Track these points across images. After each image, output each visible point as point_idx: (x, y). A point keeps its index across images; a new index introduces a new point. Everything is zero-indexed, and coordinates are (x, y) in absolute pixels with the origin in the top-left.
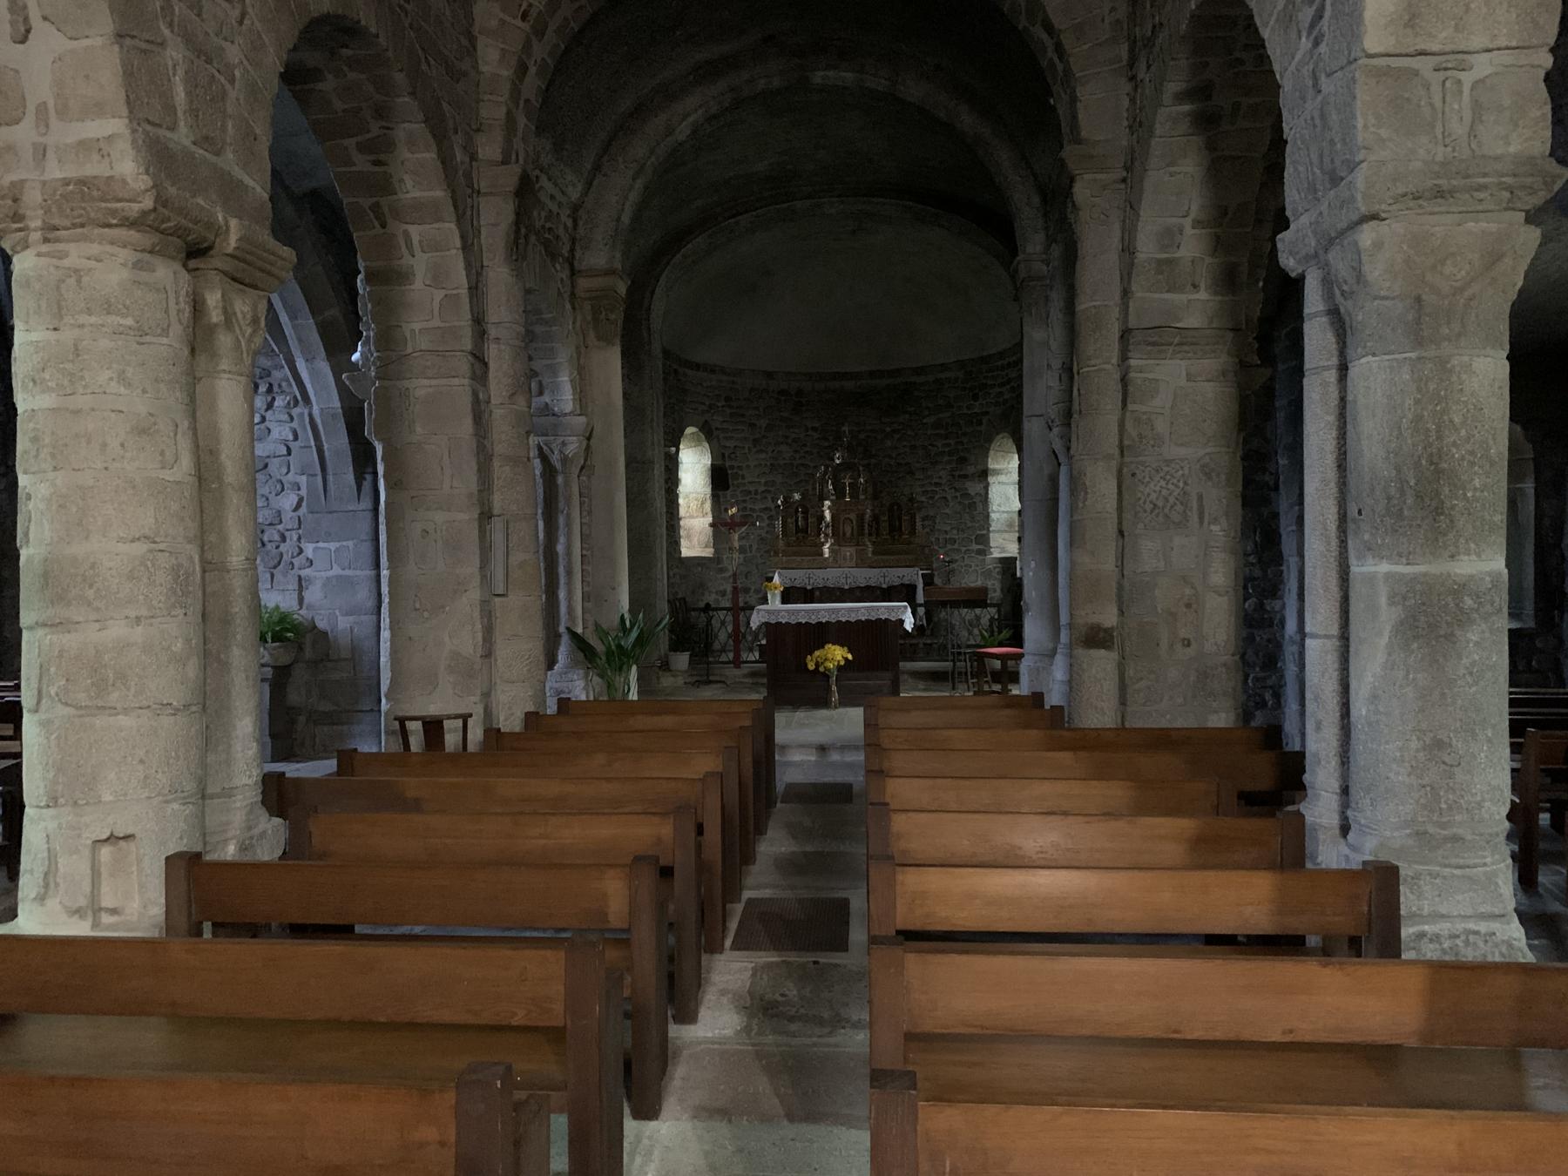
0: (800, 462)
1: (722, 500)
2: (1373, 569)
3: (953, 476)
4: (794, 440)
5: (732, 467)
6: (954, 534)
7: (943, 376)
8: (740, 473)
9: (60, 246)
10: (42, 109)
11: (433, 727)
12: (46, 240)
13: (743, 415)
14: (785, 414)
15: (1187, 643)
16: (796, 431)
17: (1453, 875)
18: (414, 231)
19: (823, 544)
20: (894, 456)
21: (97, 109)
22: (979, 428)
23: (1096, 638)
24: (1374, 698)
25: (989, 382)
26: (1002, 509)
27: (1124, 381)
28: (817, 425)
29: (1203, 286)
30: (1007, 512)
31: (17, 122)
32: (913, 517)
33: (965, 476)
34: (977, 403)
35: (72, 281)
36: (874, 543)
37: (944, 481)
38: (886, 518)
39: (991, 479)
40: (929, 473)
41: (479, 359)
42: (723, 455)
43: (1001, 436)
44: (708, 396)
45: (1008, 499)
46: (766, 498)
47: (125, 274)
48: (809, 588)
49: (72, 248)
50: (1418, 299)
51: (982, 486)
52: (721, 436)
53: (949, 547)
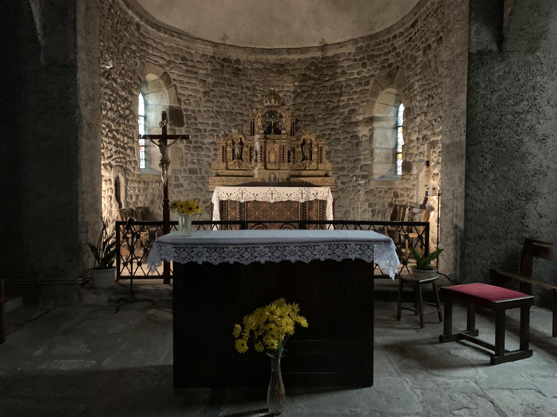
0: (237, 111)
4: (235, 95)
5: (186, 110)
6: (346, 165)
7: (340, 51)
13: (196, 73)
16: (234, 88)
19: (253, 168)
20: (303, 109)
22: (366, 88)
25: (376, 53)
26: (383, 146)
30: (386, 149)
32: (321, 150)
34: (365, 70)
37: (337, 127)
42: (179, 100)
43: (384, 92)
44: (168, 54)
45: (387, 139)
48: (242, 201)
51: (368, 129)
52: (178, 85)
53: (340, 173)
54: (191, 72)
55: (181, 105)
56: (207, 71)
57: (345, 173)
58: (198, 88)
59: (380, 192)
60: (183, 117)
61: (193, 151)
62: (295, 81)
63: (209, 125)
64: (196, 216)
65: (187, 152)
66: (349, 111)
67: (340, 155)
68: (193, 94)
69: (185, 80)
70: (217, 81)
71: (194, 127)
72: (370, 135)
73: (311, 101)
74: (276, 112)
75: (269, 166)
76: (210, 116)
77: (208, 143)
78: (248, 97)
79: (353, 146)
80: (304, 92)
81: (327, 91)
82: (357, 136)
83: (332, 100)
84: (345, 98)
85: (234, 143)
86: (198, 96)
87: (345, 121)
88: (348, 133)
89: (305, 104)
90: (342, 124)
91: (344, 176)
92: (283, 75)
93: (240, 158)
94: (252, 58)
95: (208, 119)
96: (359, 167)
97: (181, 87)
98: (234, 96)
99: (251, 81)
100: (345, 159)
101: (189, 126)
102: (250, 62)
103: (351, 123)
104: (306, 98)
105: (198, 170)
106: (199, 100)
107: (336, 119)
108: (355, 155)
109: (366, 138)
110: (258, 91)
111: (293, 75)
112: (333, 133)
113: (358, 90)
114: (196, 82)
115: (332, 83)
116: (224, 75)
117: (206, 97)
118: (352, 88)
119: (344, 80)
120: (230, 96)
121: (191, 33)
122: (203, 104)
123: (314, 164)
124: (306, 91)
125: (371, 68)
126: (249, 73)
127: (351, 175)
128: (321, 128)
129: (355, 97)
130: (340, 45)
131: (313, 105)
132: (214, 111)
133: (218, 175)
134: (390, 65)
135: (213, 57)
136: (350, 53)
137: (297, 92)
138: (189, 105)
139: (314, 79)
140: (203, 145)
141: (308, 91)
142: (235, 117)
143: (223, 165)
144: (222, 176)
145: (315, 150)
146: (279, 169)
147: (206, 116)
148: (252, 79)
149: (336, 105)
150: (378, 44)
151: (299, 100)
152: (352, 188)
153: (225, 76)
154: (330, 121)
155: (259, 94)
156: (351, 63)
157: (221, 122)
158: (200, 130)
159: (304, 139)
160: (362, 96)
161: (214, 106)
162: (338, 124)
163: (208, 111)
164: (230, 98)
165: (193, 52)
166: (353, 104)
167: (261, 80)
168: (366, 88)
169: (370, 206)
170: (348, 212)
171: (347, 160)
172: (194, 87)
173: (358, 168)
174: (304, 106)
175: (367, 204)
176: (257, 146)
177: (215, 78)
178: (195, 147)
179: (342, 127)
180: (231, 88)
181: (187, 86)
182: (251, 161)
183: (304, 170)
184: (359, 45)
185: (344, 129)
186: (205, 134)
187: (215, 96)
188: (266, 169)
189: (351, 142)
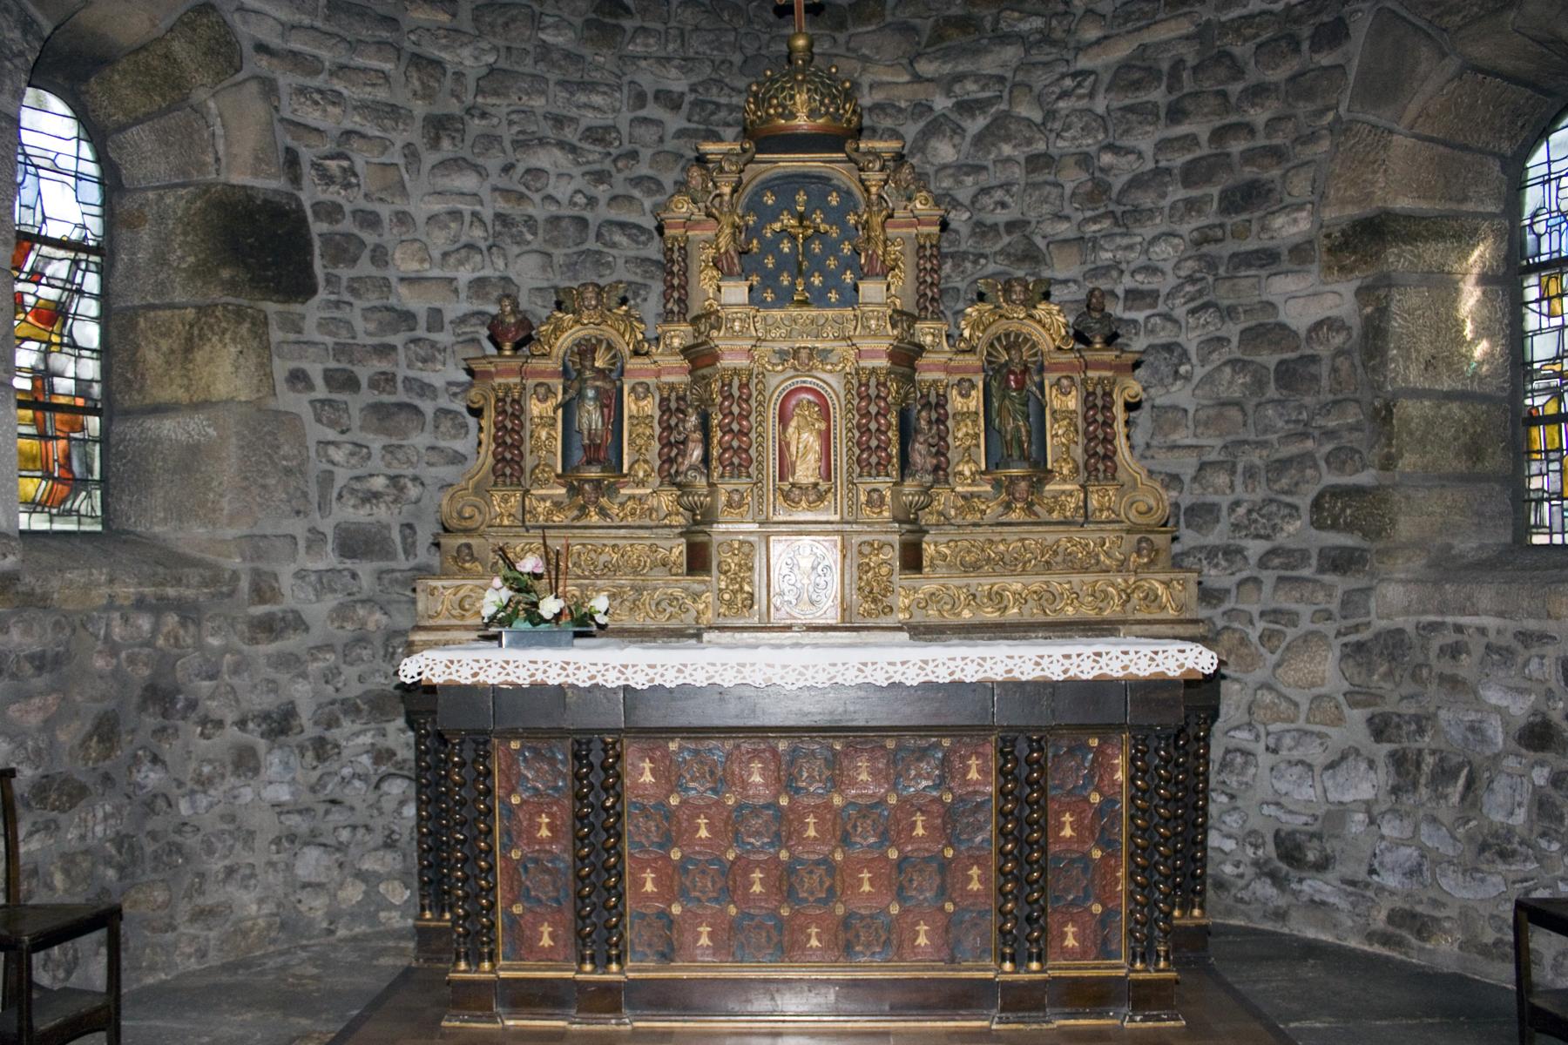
0: (614, 214)
1: (276, 335)
3: (1211, 264)
4: (597, 135)
5: (331, 211)
8: (369, 238)
13: (390, 22)
16: (597, 100)
20: (964, 195)
28: (677, 83)
37: (1163, 284)
38: (975, 401)
52: (286, 80)
53: (1189, 538)
55: (296, 180)
56: (454, 15)
57: (1217, 536)
58: (401, 97)
59: (1454, 651)
60: (308, 244)
61: (362, 428)
62: (919, 55)
63: (456, 291)
64: (385, 786)
65: (331, 435)
66: (1224, 196)
67: (1182, 437)
69: (325, 54)
70: (503, 64)
71: (373, 300)
72: (1368, 320)
73: (1007, 149)
76: (464, 239)
77: (450, 384)
78: (670, 145)
79: (1259, 384)
81: (1091, 95)
82: (1283, 327)
83: (1126, 142)
86: (399, 138)
87: (1206, 249)
88: (1229, 313)
89: (979, 169)
91: (1211, 553)
92: (852, 30)
95: (452, 260)
96: (1304, 502)
97: (302, 91)
98: (596, 141)
100: (1213, 457)
101: (347, 297)
104: (979, 140)
105: (396, 535)
106: (401, 161)
107: (1155, 240)
108: (1273, 437)
109: (1338, 340)
110: (723, 114)
111: (906, 29)
112: (1140, 316)
113: (1278, 75)
114: (388, 67)
115: (1122, 50)
116: (542, 36)
117: (446, 144)
118: (1238, 72)
119: (1192, 29)
120: (575, 141)
124: (976, 101)
126: (673, 24)
127: (1255, 548)
129: (1259, 116)
131: (1017, 173)
132: (487, 214)
137: (931, 109)
138: (347, 186)
139: (1021, 38)
140: (421, 396)
141: (990, 102)
142: (598, 246)
147: (439, 240)
148: (691, 53)
149: (1150, 165)
152: (1261, 625)
153: (548, 37)
154: (1119, 255)
155: (728, 125)
158: (408, 318)
160: (1303, 108)
161: (485, 194)
162: (1168, 267)
163: (456, 215)
164: (573, 149)
166: (1249, 157)
167: (737, 58)
169: (1380, 728)
170: (1239, 760)
172: (382, 94)
173: (1295, 508)
174: (969, 180)
175: (1357, 716)
177: (495, 48)
178: (376, 408)
179: (1191, 279)
180: (582, 98)
181: (338, 86)
185: (1200, 292)
186: (434, 336)
187: (490, 140)
189: (1245, 363)
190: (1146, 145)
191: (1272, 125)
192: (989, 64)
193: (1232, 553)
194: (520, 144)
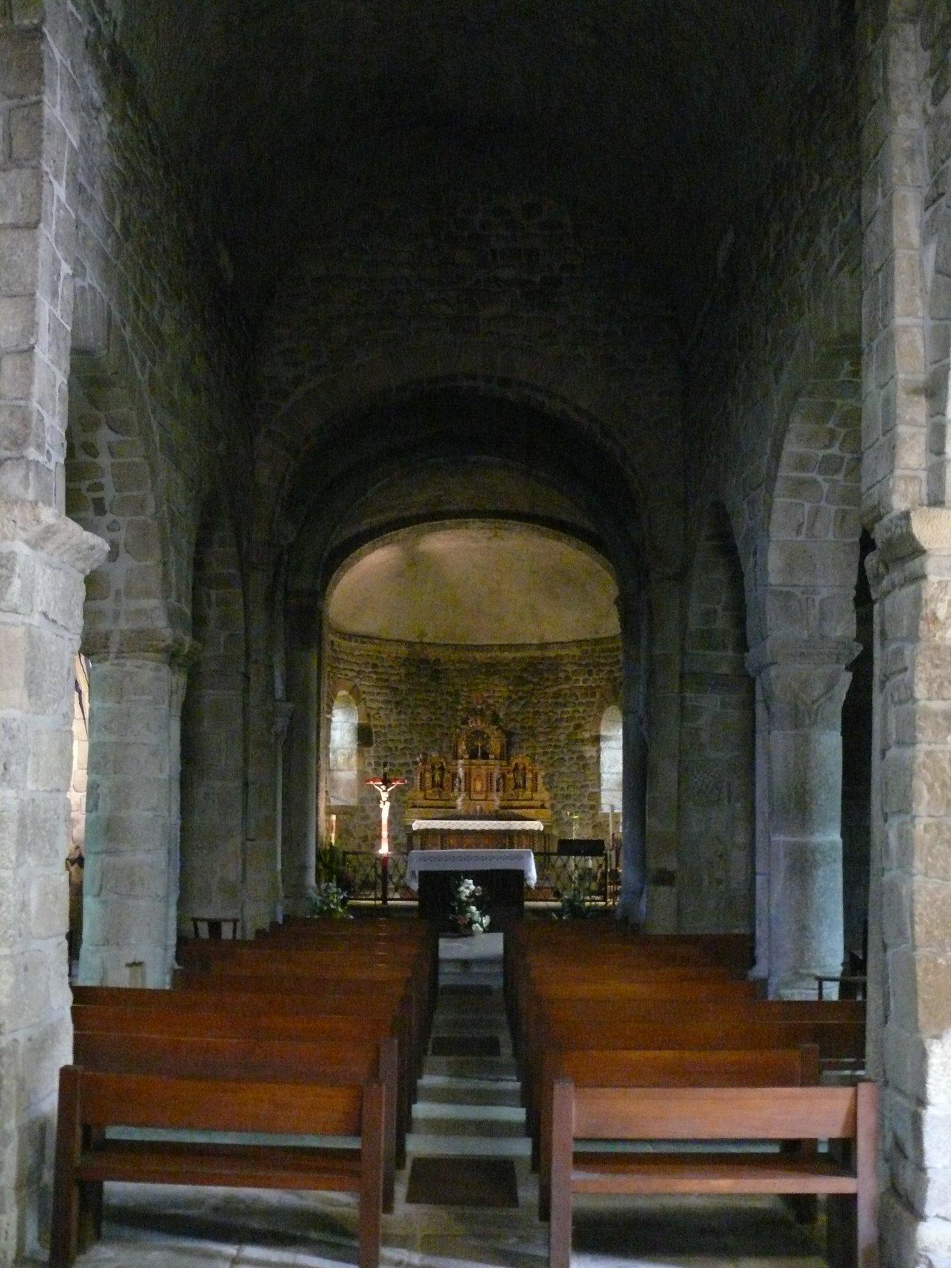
2: (778, 839)
4: (434, 703)
5: (376, 726)
6: (572, 791)
7: (564, 652)
9: (123, 661)
10: (118, 593)
11: (215, 926)
12: (117, 658)
14: (424, 680)
15: (719, 882)
17: (810, 994)
18: (213, 594)
19: (456, 798)
21: (148, 594)
23: (665, 878)
24: (778, 905)
25: (602, 661)
26: (613, 771)
27: (682, 708)
29: (730, 647)
30: (617, 773)
31: (106, 598)
33: (582, 741)
35: (128, 679)
36: (502, 800)
37: (562, 744)
39: (603, 745)
40: (550, 737)
41: (246, 677)
42: (369, 715)
46: (405, 754)
47: (151, 674)
49: (128, 663)
50: (796, 706)
51: (595, 749)
52: (368, 698)
53: (566, 802)
54: (382, 680)
55: (370, 721)
57: (571, 802)
60: (372, 734)
68: (383, 706)
74: (484, 733)
75: (474, 796)
79: (579, 769)
80: (521, 698)
84: (570, 709)
85: (433, 768)
88: (574, 752)
90: (566, 741)
93: (441, 785)
94: (454, 657)
97: (371, 700)
99: (453, 685)
102: (453, 661)
103: (577, 741)
115: (555, 689)
121: (384, 636)
122: (394, 717)
123: (528, 793)
125: (597, 677)
127: (578, 804)
128: (543, 744)
129: (581, 709)
130: (562, 644)
133: (414, 807)
134: (615, 679)
135: (407, 659)
136: (574, 656)
139: (533, 683)
143: (421, 795)
144: (420, 807)
145: (529, 776)
146: (486, 800)
147: (398, 730)
150: (603, 651)
151: (515, 709)
156: (576, 668)
157: (416, 737)
158: (391, 749)
159: (516, 764)
165: (383, 655)
168: (592, 700)
171: (574, 786)
176: (461, 772)
182: (453, 790)
183: (517, 800)
184: (584, 648)
188: (471, 799)
190: (559, 712)
191: (584, 711)
192: (526, 688)
193: (574, 805)
194: (416, 706)
